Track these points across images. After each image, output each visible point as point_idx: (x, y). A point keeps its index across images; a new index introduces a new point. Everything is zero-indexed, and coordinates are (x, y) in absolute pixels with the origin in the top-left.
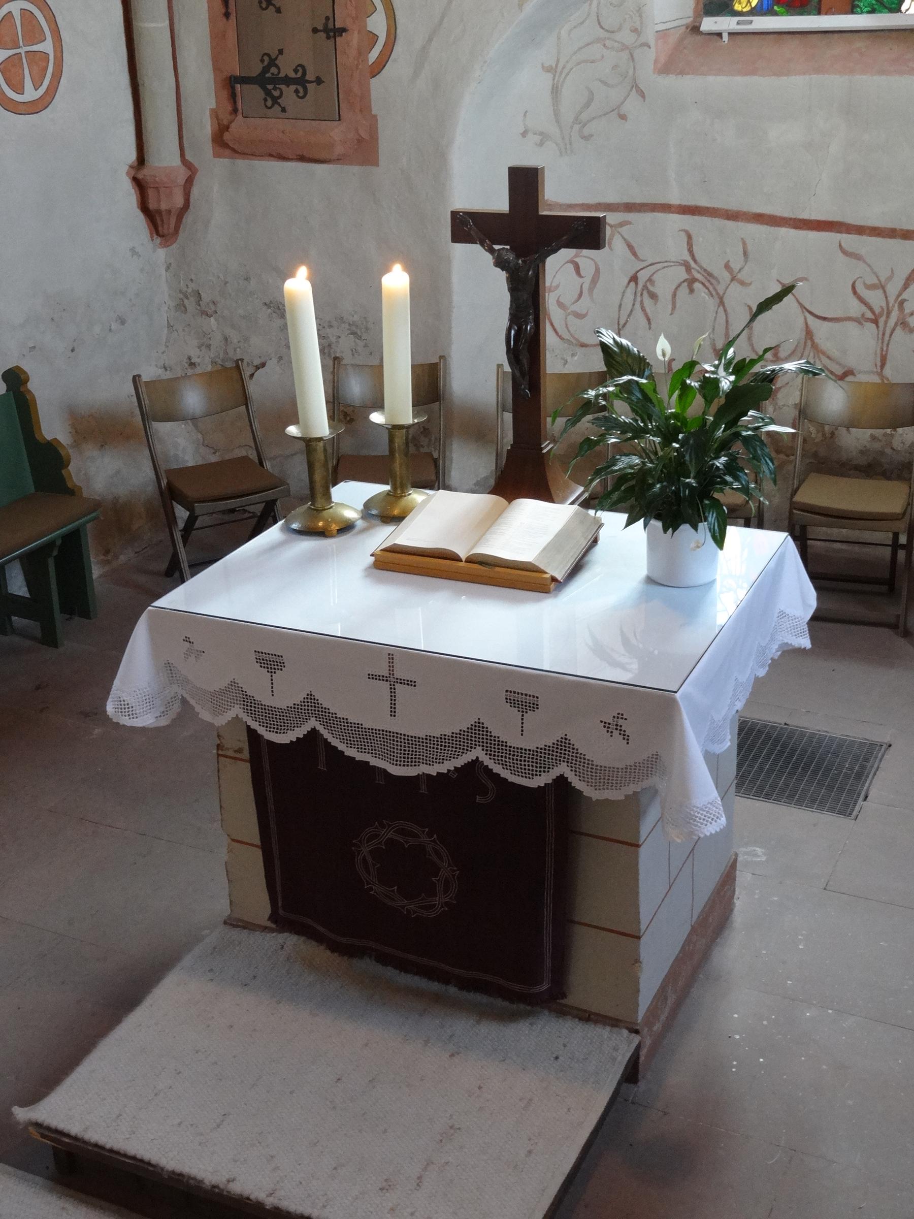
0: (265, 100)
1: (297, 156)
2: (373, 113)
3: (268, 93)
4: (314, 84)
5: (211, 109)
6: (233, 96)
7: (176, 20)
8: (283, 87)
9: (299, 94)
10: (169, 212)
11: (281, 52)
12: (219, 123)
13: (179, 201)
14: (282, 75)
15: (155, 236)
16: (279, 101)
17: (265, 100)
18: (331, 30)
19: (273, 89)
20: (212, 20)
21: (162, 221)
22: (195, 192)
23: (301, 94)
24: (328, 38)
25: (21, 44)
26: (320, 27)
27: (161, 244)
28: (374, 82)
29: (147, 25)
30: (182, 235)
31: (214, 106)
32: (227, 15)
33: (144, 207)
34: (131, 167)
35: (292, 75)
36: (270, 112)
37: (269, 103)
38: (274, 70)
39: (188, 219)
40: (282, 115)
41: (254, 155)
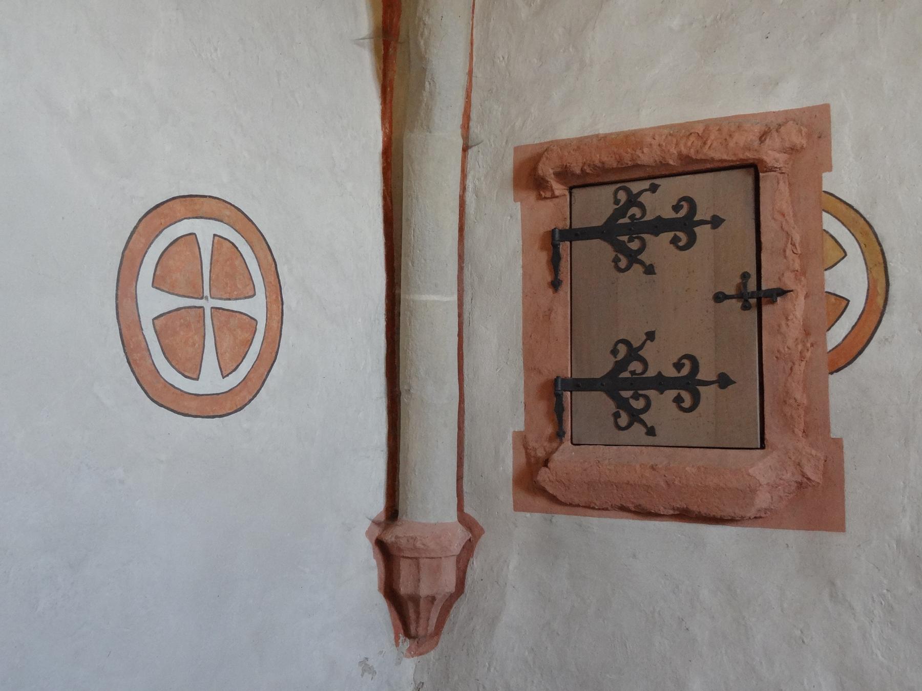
0: (617, 416)
1: (673, 509)
2: (835, 432)
3: (623, 404)
5: (516, 435)
6: (558, 412)
7: (467, 299)
8: (652, 393)
9: (683, 405)
10: (432, 599)
11: (651, 336)
12: (528, 455)
13: (449, 581)
14: (651, 373)
15: (402, 637)
16: (642, 416)
17: (617, 416)
18: (752, 295)
19: (632, 397)
20: (529, 295)
21: (418, 613)
22: (476, 565)
23: (687, 404)
24: (746, 307)
25: (207, 293)
26: (731, 291)
27: (409, 650)
28: (837, 382)
29: (425, 297)
30: (445, 638)
31: (521, 427)
32: (555, 284)
33: (390, 591)
34: (376, 523)
35: (671, 373)
36: (624, 436)
37: (624, 420)
38: (636, 366)
39: (461, 610)
40: (650, 440)
41: (589, 507)
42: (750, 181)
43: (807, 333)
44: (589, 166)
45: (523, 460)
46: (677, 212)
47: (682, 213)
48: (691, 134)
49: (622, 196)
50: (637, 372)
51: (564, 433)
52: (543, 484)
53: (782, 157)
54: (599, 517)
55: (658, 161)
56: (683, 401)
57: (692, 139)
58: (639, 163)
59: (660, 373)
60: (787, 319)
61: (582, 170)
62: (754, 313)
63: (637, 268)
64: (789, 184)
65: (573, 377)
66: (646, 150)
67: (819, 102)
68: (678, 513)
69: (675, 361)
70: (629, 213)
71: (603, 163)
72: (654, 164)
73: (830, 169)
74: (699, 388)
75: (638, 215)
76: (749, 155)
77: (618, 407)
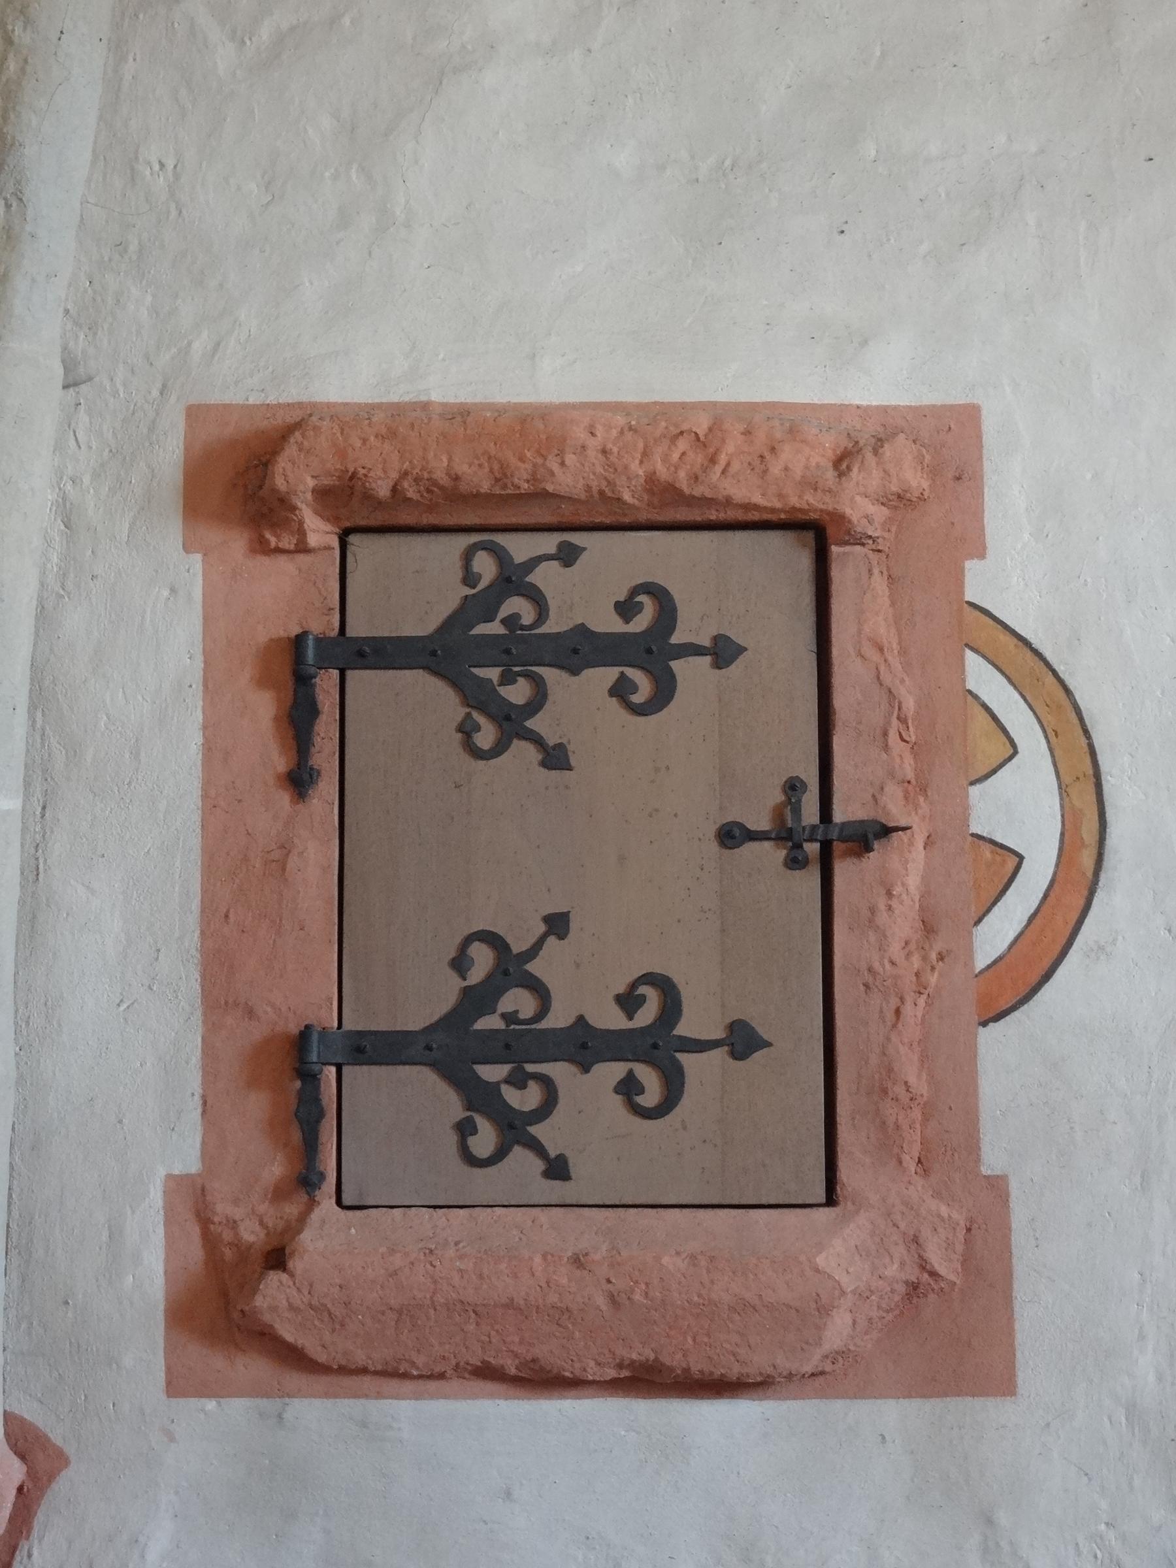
0: (465, 1129)
1: (620, 1366)
2: (993, 1160)
4: (718, 1056)
5: (176, 1185)
8: (558, 1071)
9: (640, 1100)
11: (557, 924)
12: (210, 1241)
14: (559, 1018)
17: (465, 1129)
19: (507, 1081)
23: (651, 1097)
24: (795, 862)
35: (611, 1019)
36: (484, 1183)
37: (485, 1140)
38: (518, 1001)
40: (556, 1190)
42: (804, 562)
43: (928, 928)
44: (417, 480)
45: (195, 1252)
46: (627, 621)
47: (641, 623)
48: (682, 433)
49: (486, 567)
50: (522, 1016)
51: (322, 1176)
52: (267, 1318)
53: (880, 513)
54: (417, 1396)
55: (595, 490)
56: (641, 1091)
57: (682, 445)
58: (550, 488)
59: (581, 1019)
60: (889, 894)
61: (394, 490)
62: (810, 880)
63: (523, 753)
64: (890, 576)
65: (348, 1026)
66: (570, 459)
67: (957, 397)
68: (625, 1373)
69: (621, 989)
70: (504, 611)
71: (457, 478)
72: (583, 496)
73: (982, 555)
74: (682, 1057)
75: (528, 618)
76: (813, 502)
77: (469, 1107)
